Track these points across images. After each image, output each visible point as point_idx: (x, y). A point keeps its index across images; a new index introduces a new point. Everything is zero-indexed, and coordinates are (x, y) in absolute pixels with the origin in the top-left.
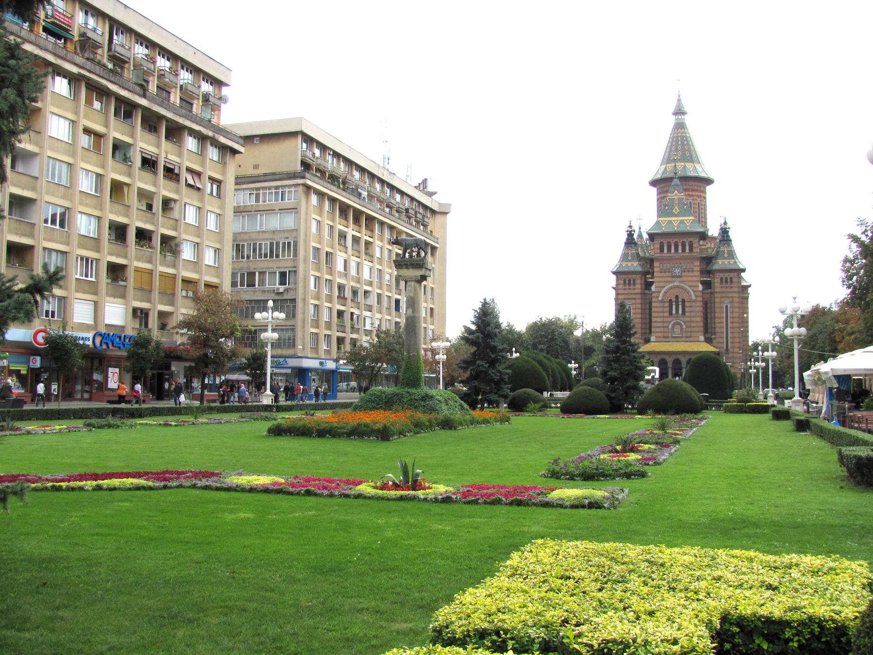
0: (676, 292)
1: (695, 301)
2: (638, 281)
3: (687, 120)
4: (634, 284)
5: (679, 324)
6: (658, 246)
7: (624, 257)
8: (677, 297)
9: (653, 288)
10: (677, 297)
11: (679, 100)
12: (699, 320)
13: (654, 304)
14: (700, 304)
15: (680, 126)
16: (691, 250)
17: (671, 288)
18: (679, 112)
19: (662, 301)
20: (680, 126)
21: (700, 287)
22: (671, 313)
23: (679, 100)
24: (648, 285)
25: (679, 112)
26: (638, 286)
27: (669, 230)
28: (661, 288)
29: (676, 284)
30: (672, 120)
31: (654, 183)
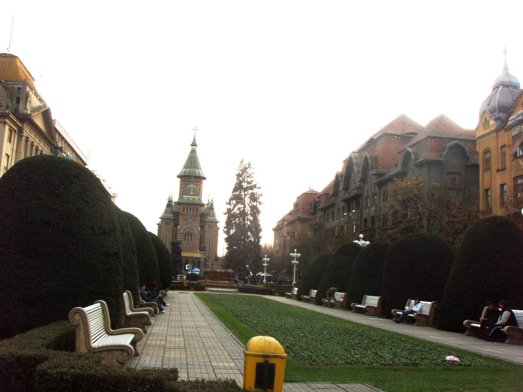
0: (188, 230)
1: (197, 235)
2: (172, 223)
3: (198, 149)
4: (170, 224)
5: (188, 244)
6: (182, 208)
7: (166, 212)
8: (189, 232)
9: (178, 227)
10: (189, 232)
11: (194, 139)
12: (197, 242)
13: (178, 235)
14: (199, 236)
15: (193, 152)
16: (197, 211)
17: (186, 228)
18: (194, 144)
19: (182, 234)
20: (193, 152)
21: (200, 229)
22: (185, 239)
23: (194, 139)
24: (176, 225)
25: (194, 144)
26: (171, 226)
27: (188, 202)
28: (182, 228)
29: (189, 226)
30: (190, 148)
31: (179, 177)
